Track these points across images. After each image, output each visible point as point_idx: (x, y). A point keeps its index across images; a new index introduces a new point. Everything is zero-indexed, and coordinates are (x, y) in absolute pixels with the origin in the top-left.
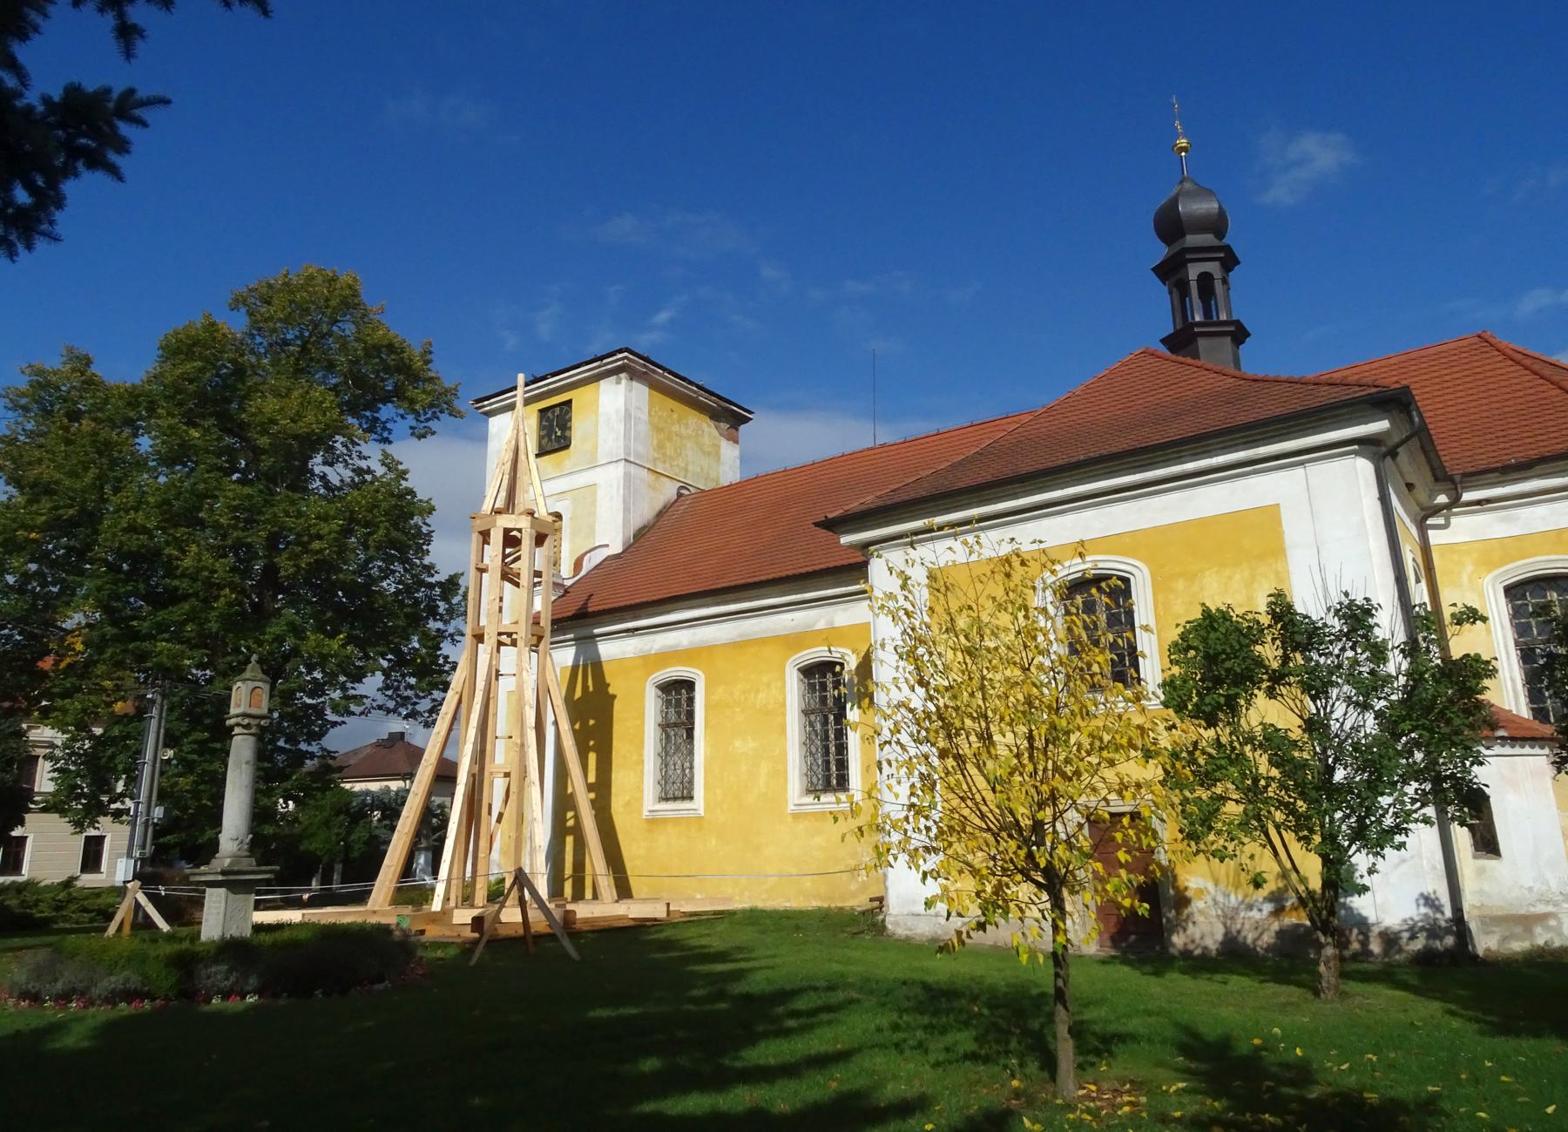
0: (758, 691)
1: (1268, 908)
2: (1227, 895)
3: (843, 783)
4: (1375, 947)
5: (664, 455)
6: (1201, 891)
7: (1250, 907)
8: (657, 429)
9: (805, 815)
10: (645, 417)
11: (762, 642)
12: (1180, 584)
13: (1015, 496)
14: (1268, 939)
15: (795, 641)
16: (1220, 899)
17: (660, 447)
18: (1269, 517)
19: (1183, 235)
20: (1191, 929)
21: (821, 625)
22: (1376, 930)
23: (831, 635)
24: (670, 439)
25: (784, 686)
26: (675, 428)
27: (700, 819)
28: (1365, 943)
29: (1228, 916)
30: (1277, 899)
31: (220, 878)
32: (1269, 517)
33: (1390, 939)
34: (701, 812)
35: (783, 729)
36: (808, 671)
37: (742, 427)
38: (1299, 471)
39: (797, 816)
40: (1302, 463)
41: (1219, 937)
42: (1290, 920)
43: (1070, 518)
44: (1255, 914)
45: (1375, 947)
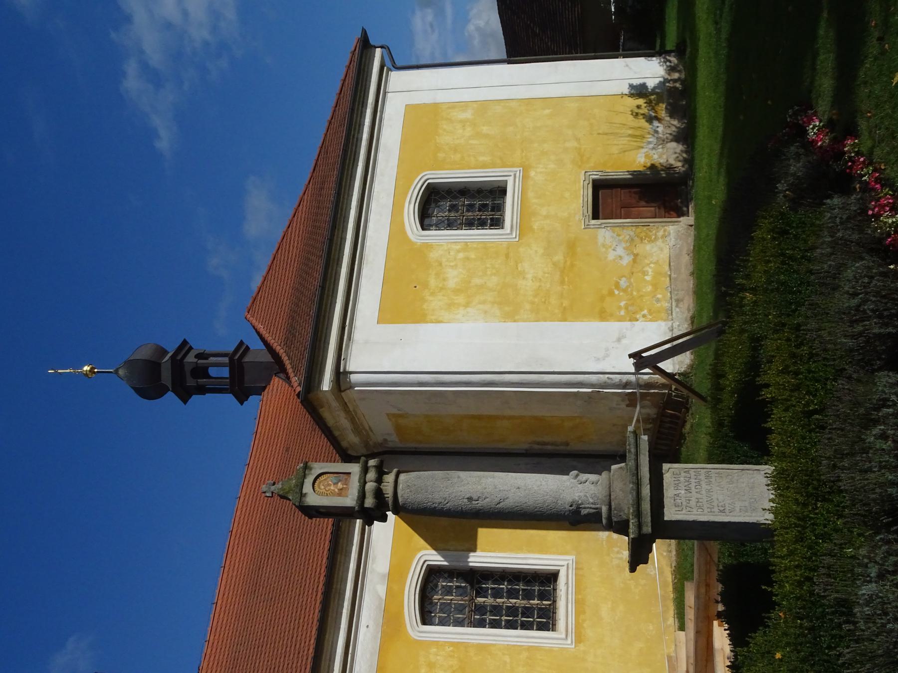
1: (656, 123)
2: (650, 143)
3: (549, 578)
4: (676, 76)
6: (647, 156)
7: (657, 132)
9: (578, 625)
12: (441, 155)
13: (343, 239)
14: (675, 122)
16: (651, 146)
18: (412, 111)
19: (159, 365)
20: (672, 161)
21: (382, 590)
22: (667, 76)
23: (395, 575)
25: (436, 643)
28: (675, 81)
29: (663, 142)
30: (650, 120)
32: (412, 111)
33: (672, 69)
35: (482, 648)
36: (426, 618)
38: (389, 95)
39: (579, 639)
40: (385, 93)
41: (674, 144)
42: (663, 114)
43: (373, 217)
44: (660, 129)
45: (676, 76)
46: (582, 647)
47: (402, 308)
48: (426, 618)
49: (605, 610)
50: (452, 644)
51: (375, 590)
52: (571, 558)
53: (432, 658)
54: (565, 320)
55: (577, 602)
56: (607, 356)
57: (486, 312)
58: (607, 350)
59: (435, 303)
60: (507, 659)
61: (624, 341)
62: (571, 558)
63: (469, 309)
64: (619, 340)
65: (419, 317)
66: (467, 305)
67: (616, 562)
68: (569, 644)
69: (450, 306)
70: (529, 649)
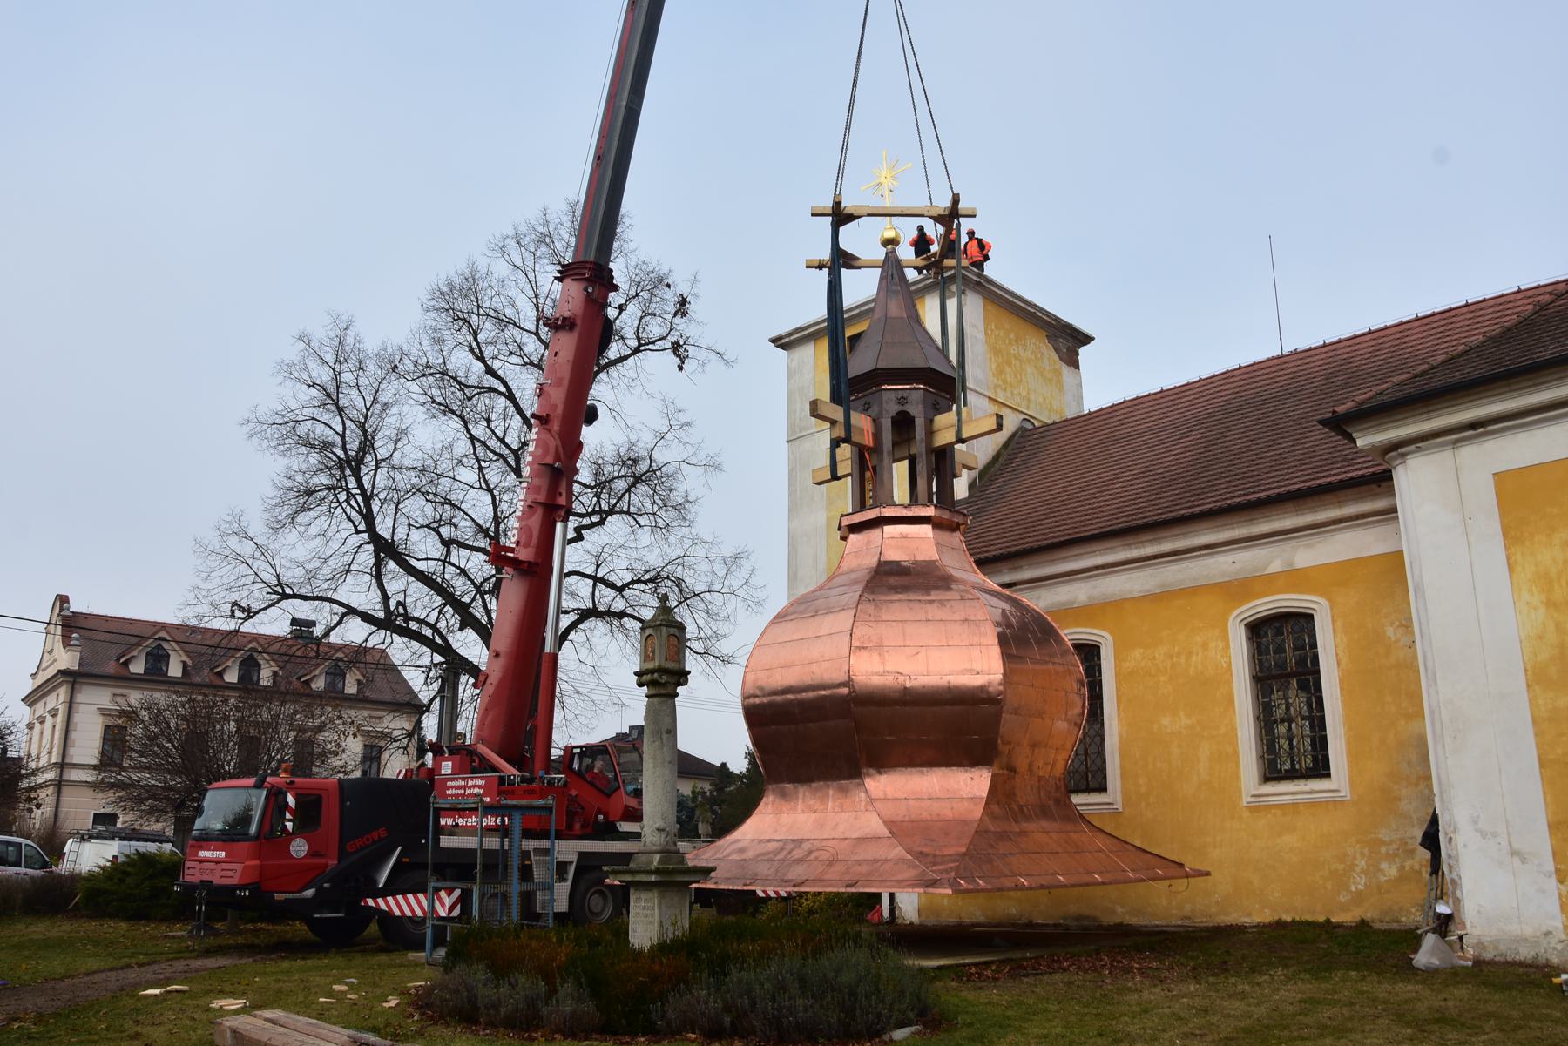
0: (1190, 654)
5: (1004, 381)
8: (996, 352)
9: (1269, 807)
10: (981, 336)
11: (1194, 591)
15: (1240, 589)
17: (999, 372)
21: (1276, 567)
23: (1295, 579)
24: (1009, 363)
25: (1227, 646)
26: (1014, 350)
27: (1116, 813)
31: (653, 878)
34: (1119, 806)
36: (1256, 629)
37: (1083, 351)
39: (1254, 809)
46: (1246, 814)
47: (1521, 499)
48: (1256, 629)
49: (1289, 840)
50: (1229, 665)
51: (1272, 559)
52: (1345, 793)
53: (1213, 645)
54: (1542, 765)
55: (1295, 805)
56: (1483, 834)
57: (1540, 638)
58: (1494, 835)
59: (1548, 554)
60: (1223, 730)
61: (1516, 860)
62: (1345, 793)
63: (1542, 610)
64: (1513, 853)
65: (1513, 534)
66: (1550, 604)
67: (1350, 851)
68: (1246, 799)
69: (1545, 580)
70: (1236, 753)
